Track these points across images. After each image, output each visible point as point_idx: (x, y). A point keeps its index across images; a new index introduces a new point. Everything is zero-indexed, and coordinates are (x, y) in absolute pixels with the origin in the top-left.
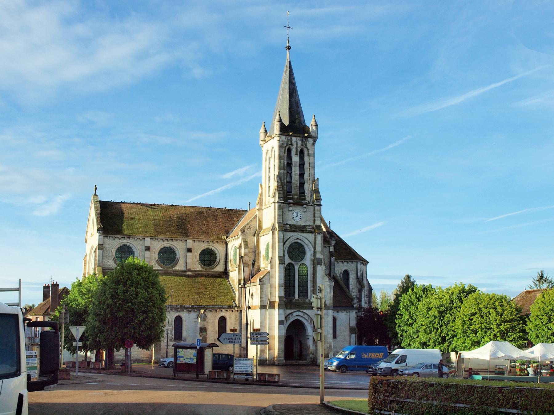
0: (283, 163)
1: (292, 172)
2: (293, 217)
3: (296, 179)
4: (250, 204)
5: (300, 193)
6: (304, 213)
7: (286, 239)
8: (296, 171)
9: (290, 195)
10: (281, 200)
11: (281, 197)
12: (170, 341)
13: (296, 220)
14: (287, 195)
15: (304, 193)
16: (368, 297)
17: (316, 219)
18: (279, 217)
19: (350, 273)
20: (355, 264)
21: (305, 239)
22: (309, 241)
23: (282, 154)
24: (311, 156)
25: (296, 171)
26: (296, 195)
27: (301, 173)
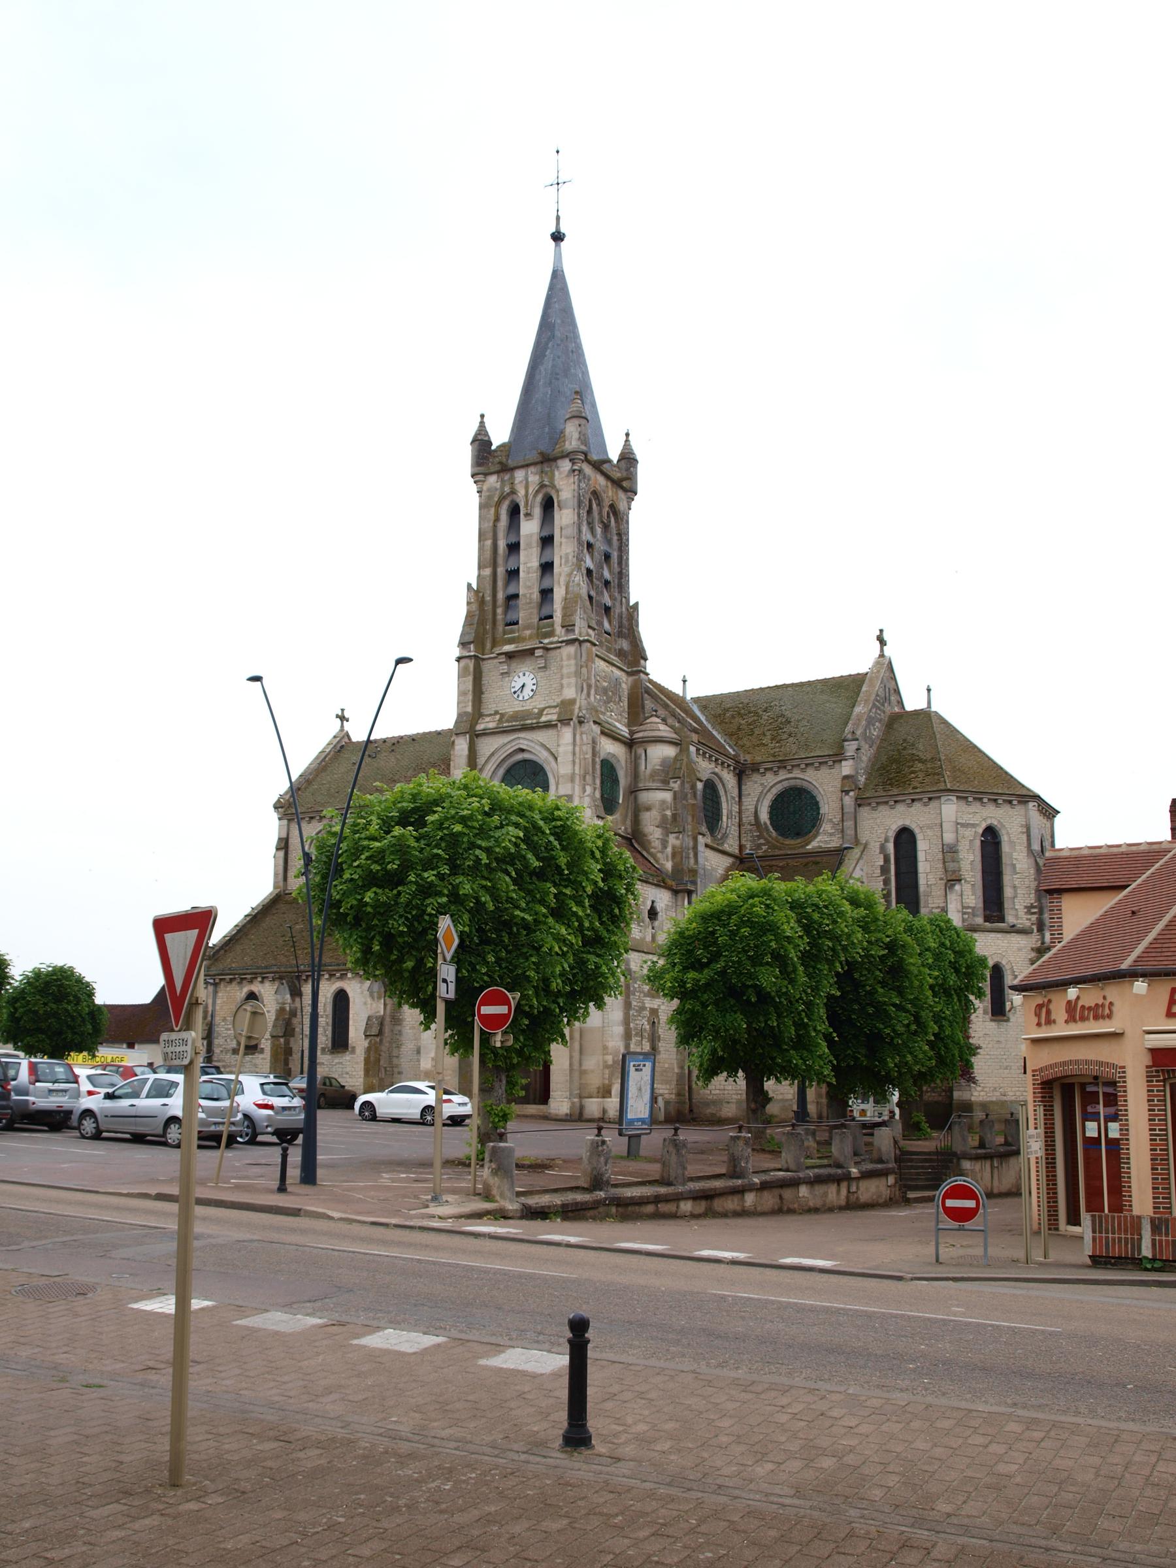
0: (489, 548)
1: (518, 569)
2: (513, 690)
3: (529, 584)
4: (684, 681)
5: (541, 619)
6: (542, 674)
7: (488, 754)
8: (529, 560)
9: (512, 632)
10: (470, 651)
11: (470, 643)
12: (322, 1054)
13: (521, 698)
14: (505, 633)
15: (551, 617)
16: (1035, 910)
17: (565, 681)
18: (462, 698)
19: (919, 837)
20: (934, 804)
21: (538, 748)
22: (548, 750)
23: (486, 525)
24: (567, 508)
25: (529, 560)
26: (527, 627)
27: (543, 561)
